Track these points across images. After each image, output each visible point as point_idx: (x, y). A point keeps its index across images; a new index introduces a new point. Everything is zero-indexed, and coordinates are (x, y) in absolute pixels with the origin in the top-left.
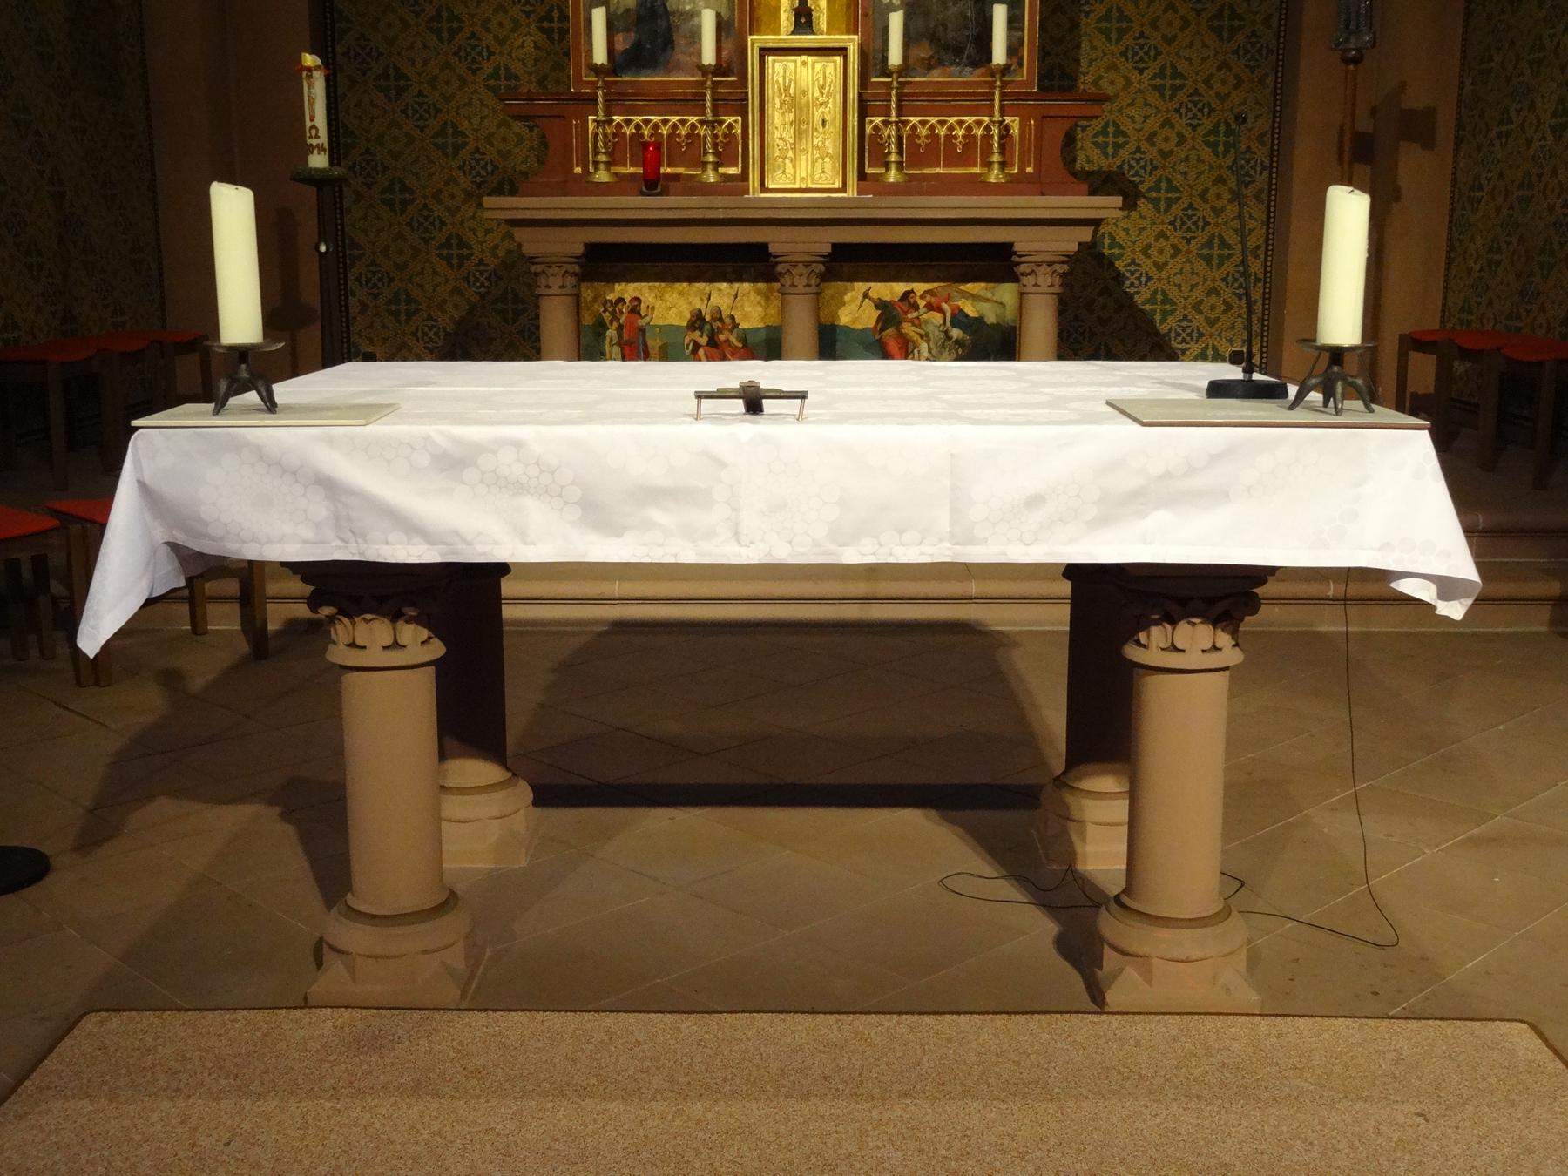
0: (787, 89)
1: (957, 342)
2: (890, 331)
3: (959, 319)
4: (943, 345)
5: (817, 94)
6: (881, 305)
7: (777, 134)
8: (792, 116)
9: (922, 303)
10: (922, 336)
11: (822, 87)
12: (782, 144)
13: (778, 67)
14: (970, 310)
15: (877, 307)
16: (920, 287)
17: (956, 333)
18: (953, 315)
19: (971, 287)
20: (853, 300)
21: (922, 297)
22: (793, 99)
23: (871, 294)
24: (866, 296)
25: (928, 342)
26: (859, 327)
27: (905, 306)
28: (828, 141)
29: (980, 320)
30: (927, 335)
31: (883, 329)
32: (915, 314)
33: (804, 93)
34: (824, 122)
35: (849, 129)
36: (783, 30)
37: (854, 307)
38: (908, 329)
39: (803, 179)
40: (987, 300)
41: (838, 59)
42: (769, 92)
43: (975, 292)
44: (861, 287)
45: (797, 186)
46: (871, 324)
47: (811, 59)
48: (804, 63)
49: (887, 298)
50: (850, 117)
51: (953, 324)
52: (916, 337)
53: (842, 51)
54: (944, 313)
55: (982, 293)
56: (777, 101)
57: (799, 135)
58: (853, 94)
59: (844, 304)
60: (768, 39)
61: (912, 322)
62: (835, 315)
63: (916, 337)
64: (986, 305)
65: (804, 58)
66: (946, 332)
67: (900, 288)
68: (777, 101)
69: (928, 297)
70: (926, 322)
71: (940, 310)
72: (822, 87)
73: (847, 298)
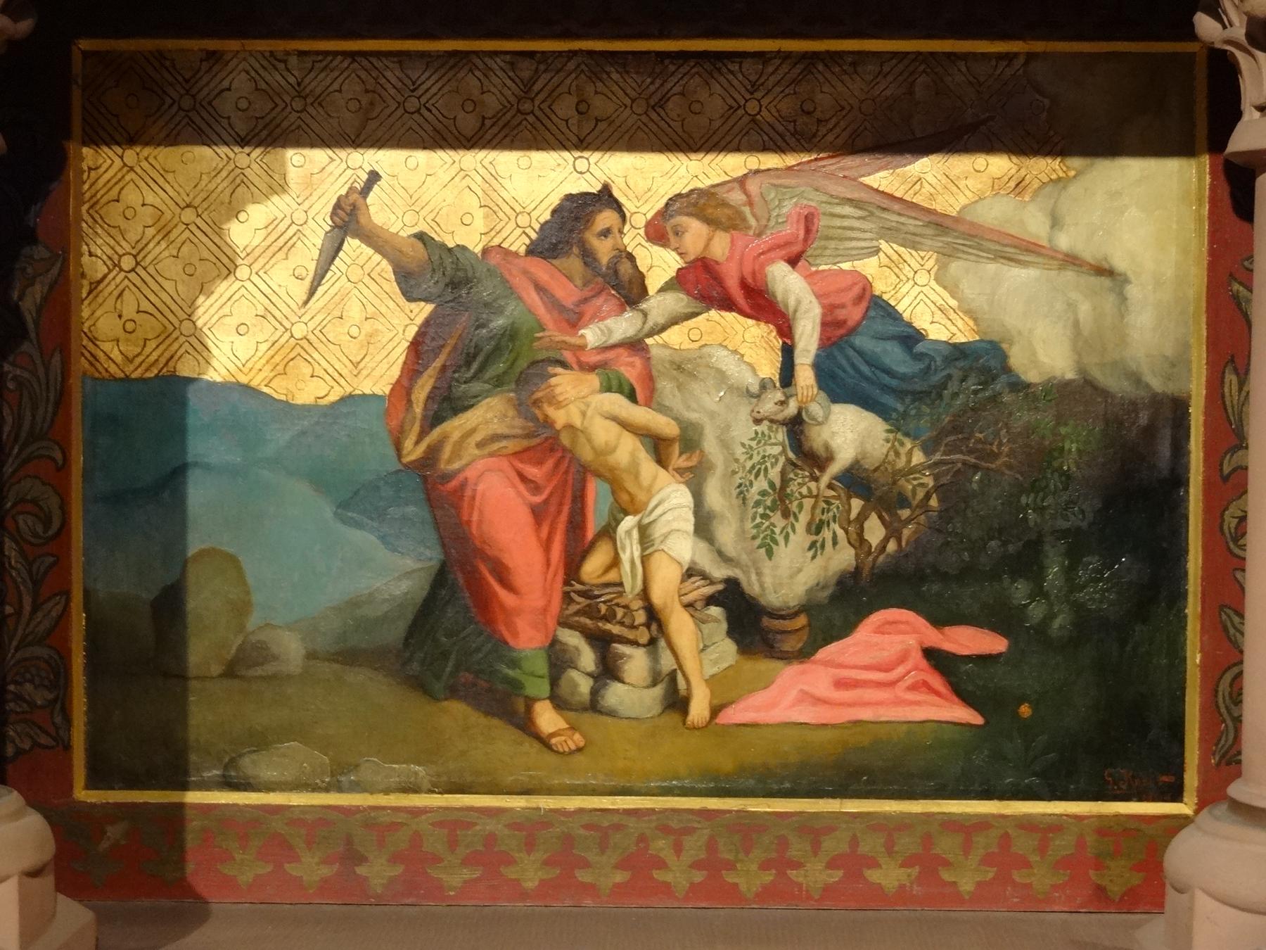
1: (856, 480)
2: (488, 415)
3: (864, 356)
4: (781, 499)
6: (436, 272)
9: (659, 265)
10: (658, 447)
14: (930, 303)
15: (408, 283)
16: (646, 179)
17: (850, 432)
18: (835, 334)
19: (934, 178)
20: (280, 243)
21: (658, 233)
23: (383, 211)
24: (348, 219)
25: (695, 479)
26: (309, 389)
27: (563, 277)
29: (982, 362)
30: (689, 439)
31: (447, 404)
32: (623, 325)
37: (285, 278)
38: (584, 407)
40: (1017, 249)
43: (949, 204)
44: (317, 174)
46: (380, 376)
49: (469, 236)
51: (839, 382)
52: (628, 452)
54: (785, 329)
55: (996, 213)
59: (226, 264)
61: (599, 366)
62: (179, 330)
63: (627, 450)
64: (1020, 277)
66: (796, 426)
67: (536, 180)
69: (695, 232)
70: (683, 367)
71: (760, 303)
73: (244, 232)
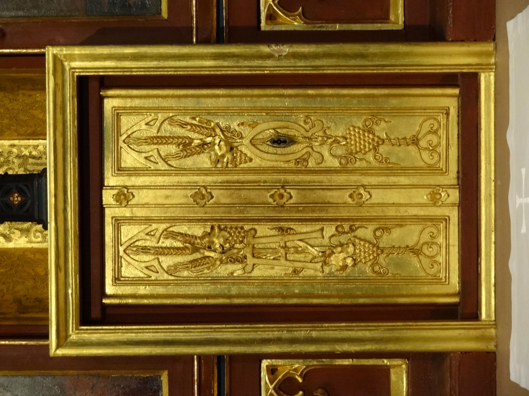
0: (191, 244)
5: (204, 161)
7: (312, 270)
8: (263, 229)
11: (186, 146)
12: (337, 259)
13: (133, 271)
22: (218, 224)
28: (332, 132)
33: (201, 196)
34: (280, 141)
35: (302, 67)
36: (44, 245)
39: (435, 200)
41: (112, 102)
42: (194, 291)
45: (454, 215)
47: (111, 179)
48: (124, 196)
50: (268, 67)
53: (90, 90)
56: (224, 270)
57: (315, 212)
58: (201, 58)
60: (59, 291)
65: (108, 197)
68: (224, 270)
72: (186, 146)
